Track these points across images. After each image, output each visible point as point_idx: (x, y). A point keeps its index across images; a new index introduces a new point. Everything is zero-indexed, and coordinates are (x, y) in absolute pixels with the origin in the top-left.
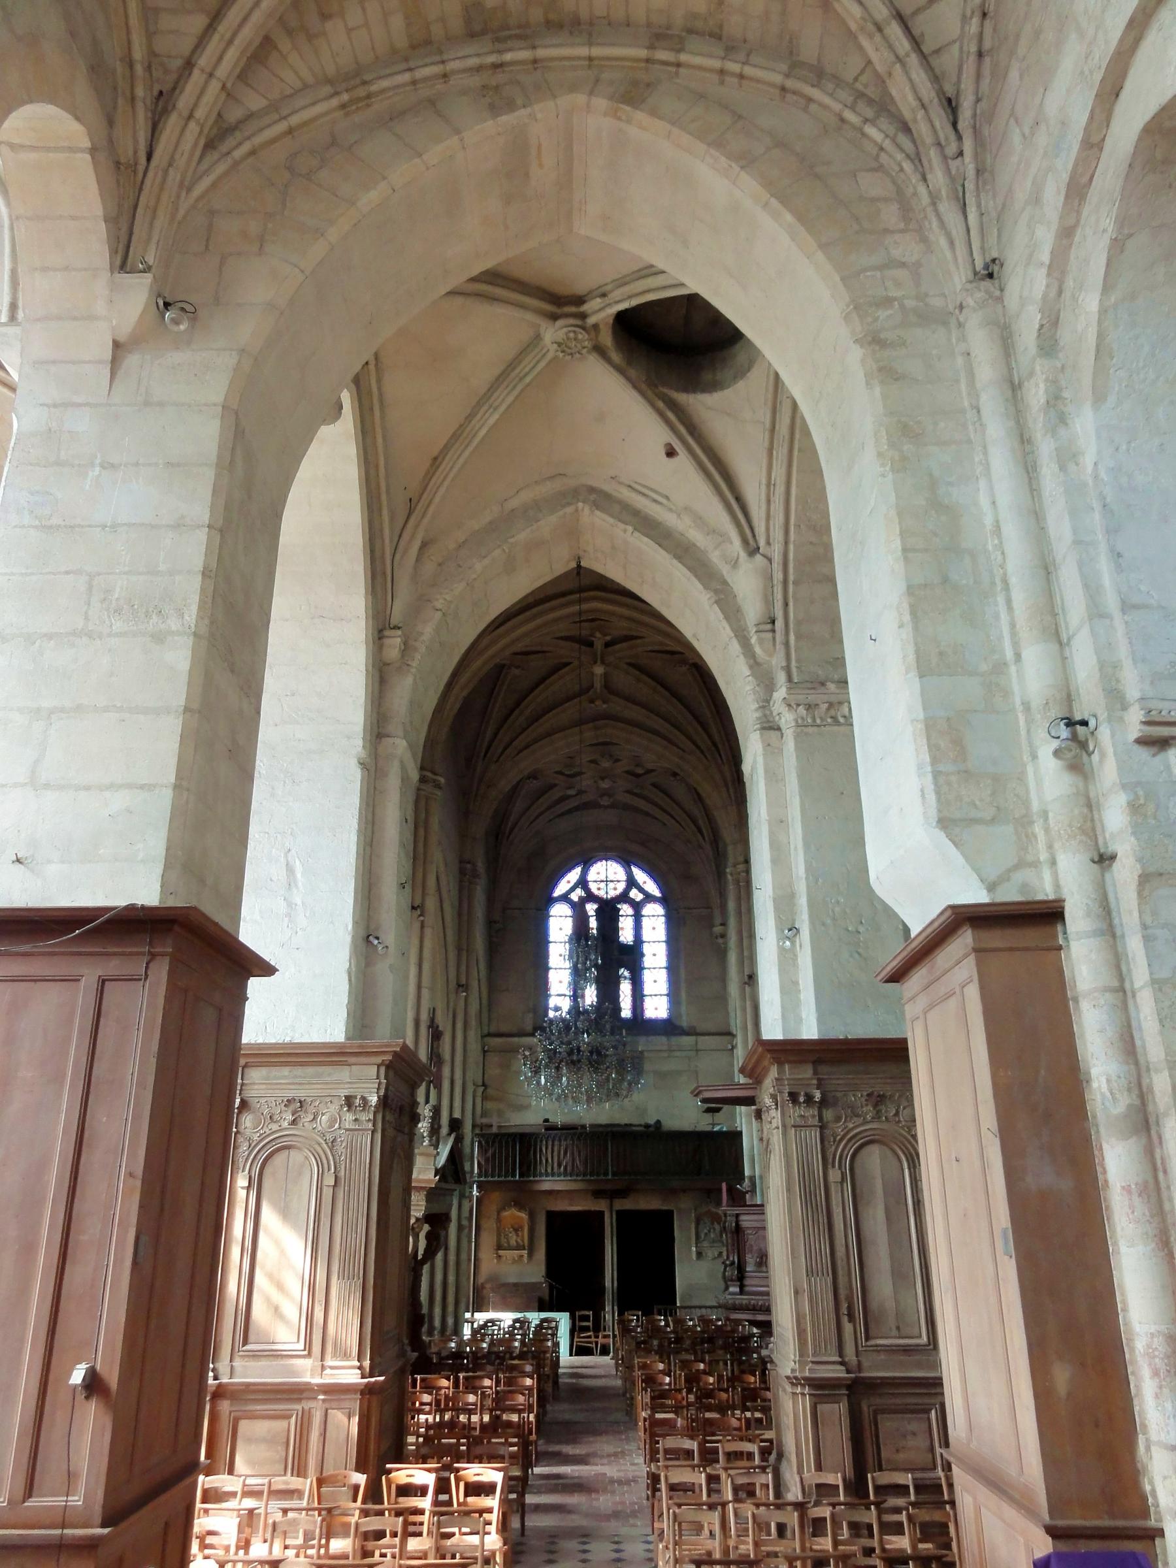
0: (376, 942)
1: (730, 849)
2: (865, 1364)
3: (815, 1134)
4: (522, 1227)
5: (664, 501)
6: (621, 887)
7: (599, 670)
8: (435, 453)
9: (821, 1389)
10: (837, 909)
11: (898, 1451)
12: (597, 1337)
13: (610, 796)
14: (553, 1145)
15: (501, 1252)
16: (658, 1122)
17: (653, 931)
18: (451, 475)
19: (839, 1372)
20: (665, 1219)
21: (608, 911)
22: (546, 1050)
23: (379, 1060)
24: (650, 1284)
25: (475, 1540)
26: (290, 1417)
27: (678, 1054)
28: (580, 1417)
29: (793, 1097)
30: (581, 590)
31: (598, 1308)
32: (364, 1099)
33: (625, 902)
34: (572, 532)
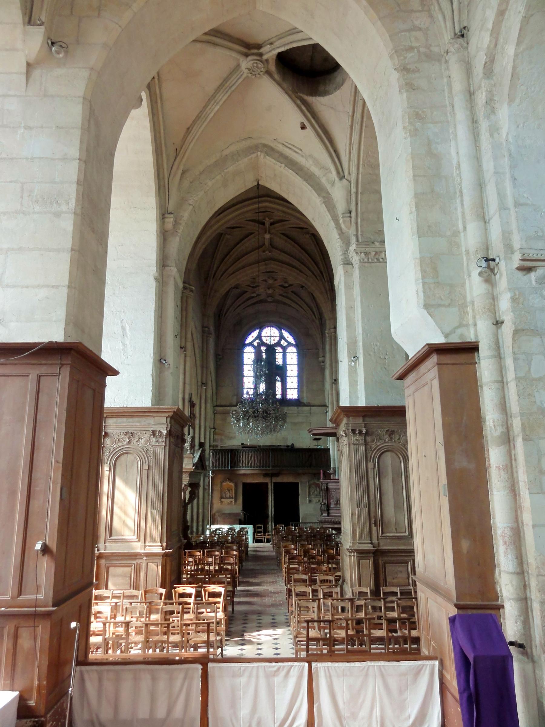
0: (164, 362)
1: (327, 322)
2: (381, 544)
3: (363, 448)
5: (300, 152)
6: (277, 339)
7: (267, 236)
8: (188, 127)
9: (362, 554)
10: (376, 348)
11: (394, 579)
12: (265, 535)
13: (272, 297)
15: (223, 500)
16: (293, 444)
17: (290, 360)
18: (196, 137)
19: (369, 547)
20: (295, 486)
21: (271, 350)
22: (243, 411)
23: (167, 415)
24: (288, 513)
25: (213, 614)
26: (131, 566)
28: (258, 567)
29: (353, 431)
30: (259, 197)
31: (265, 523)
32: (160, 432)
34: (255, 167)
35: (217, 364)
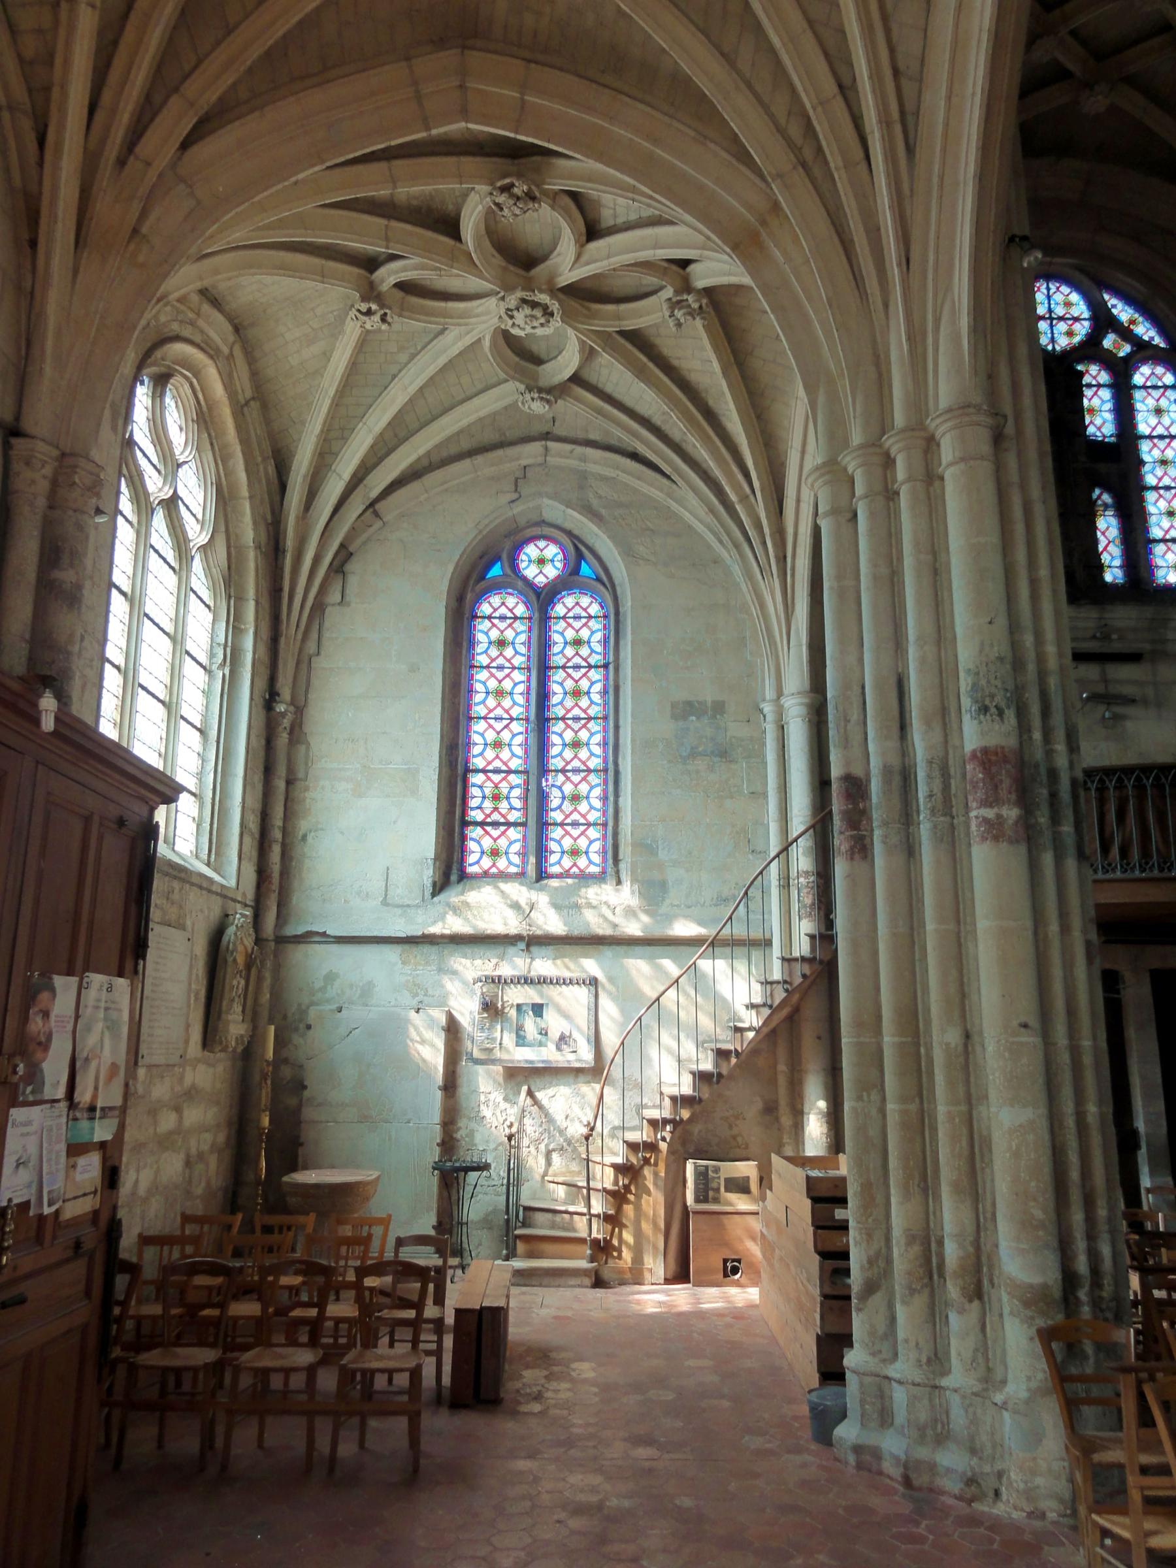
6: (1082, 330)
21: (1061, 376)
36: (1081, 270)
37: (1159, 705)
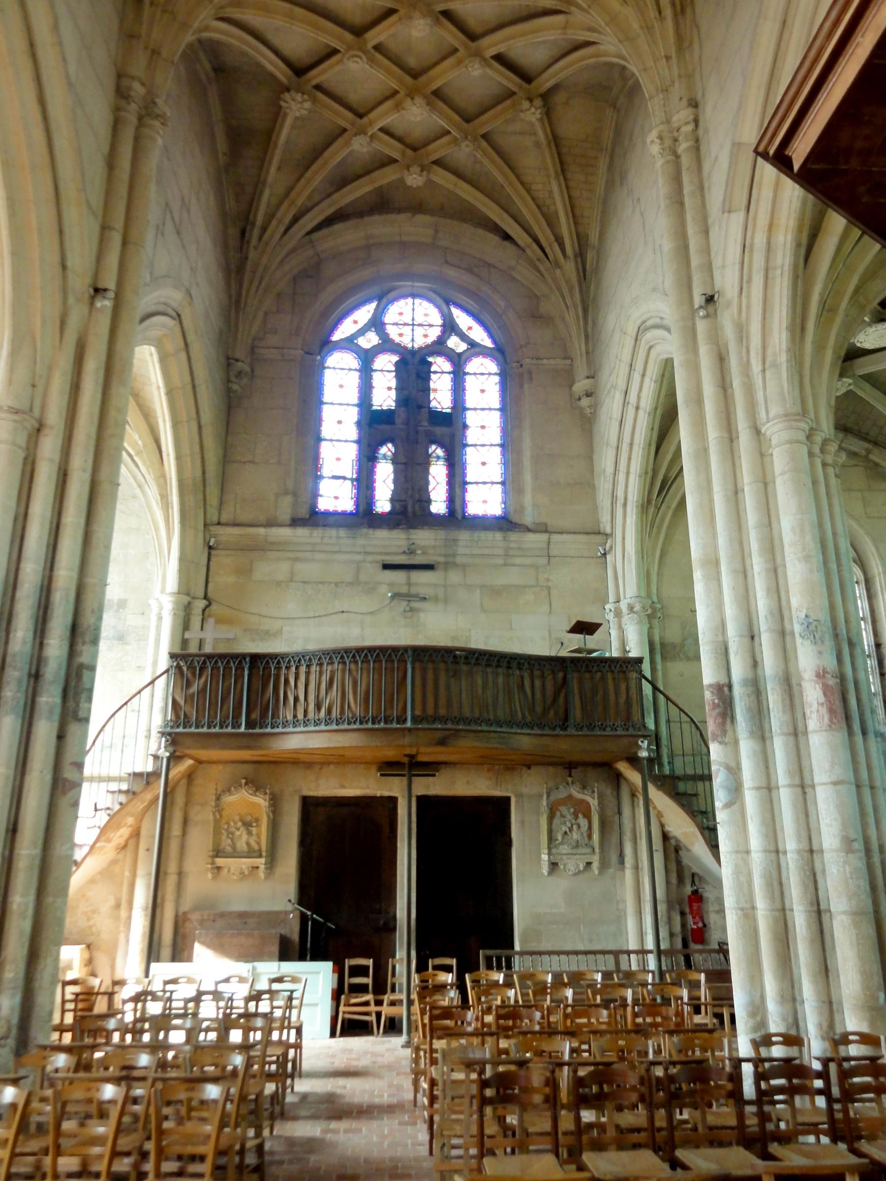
4: (257, 820)
6: (434, 333)
12: (379, 1003)
14: (308, 674)
15: (220, 861)
24: (469, 912)
27: (518, 561)
31: (382, 954)
33: (439, 354)
35: (229, 390)
36: (434, 292)
37: (446, 601)
